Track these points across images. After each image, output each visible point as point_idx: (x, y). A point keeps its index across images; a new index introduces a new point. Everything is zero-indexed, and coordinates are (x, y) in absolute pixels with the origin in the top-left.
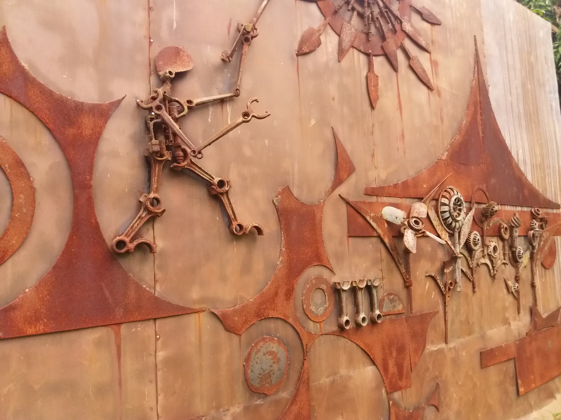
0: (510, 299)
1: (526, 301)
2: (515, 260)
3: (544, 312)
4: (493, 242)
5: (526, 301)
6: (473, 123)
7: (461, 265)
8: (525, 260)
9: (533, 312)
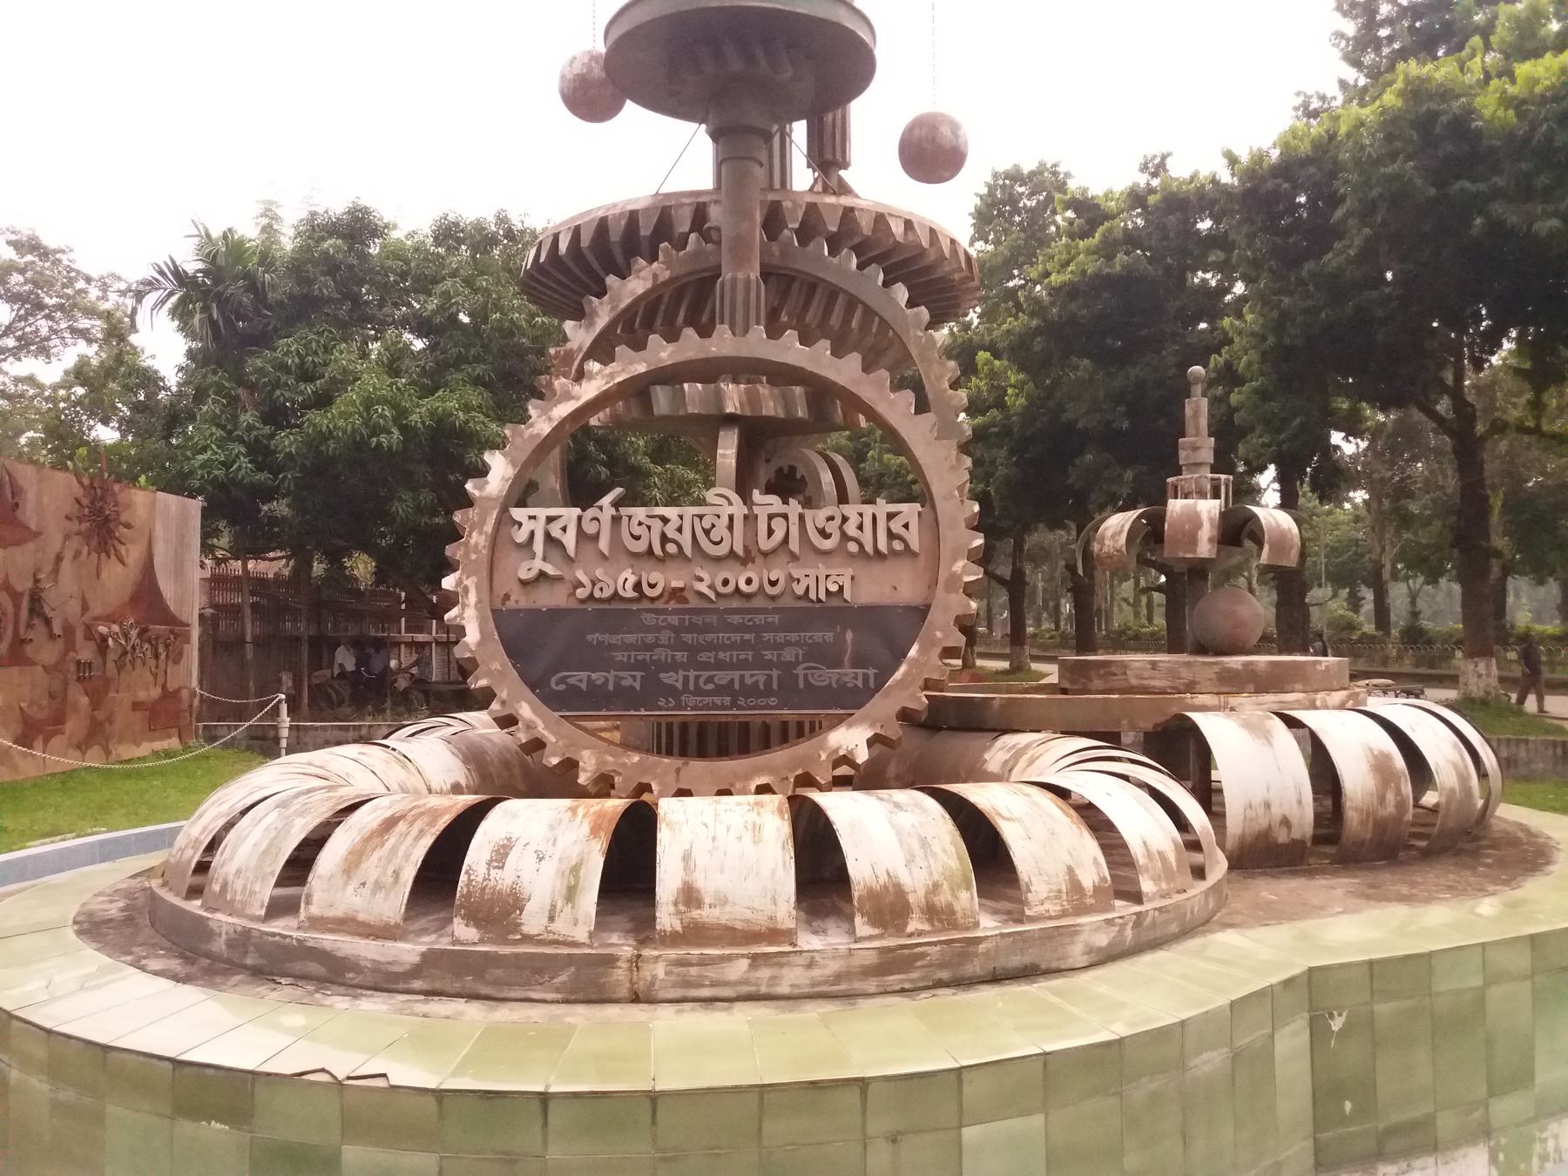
1: (161, 680)
2: (157, 656)
3: (171, 687)
4: (146, 646)
5: (161, 680)
8: (163, 657)
9: (164, 687)
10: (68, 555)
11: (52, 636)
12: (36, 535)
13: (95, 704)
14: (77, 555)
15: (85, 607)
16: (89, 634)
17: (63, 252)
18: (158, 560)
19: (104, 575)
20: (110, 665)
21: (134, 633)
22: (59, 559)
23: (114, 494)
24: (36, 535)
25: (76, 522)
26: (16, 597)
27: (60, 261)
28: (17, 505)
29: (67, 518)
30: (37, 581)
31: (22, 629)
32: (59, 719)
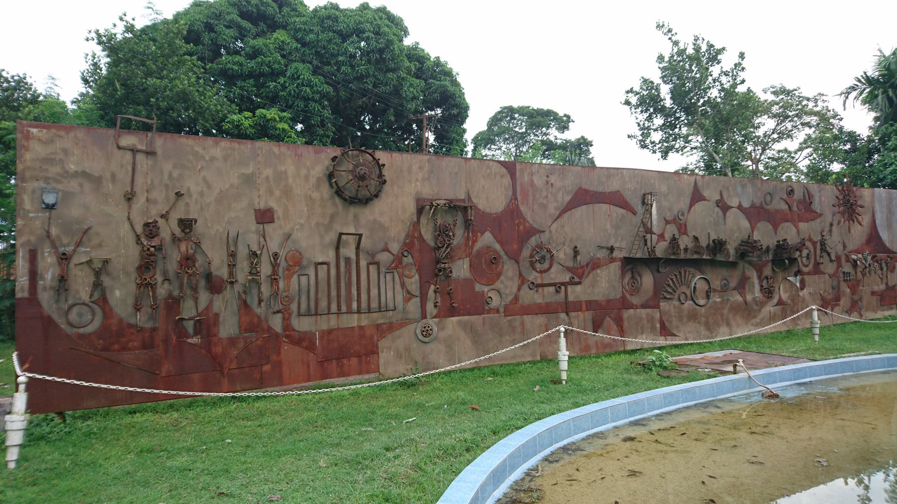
0: (880, 279)
1: (885, 281)
2: (882, 269)
3: (890, 284)
4: (876, 264)
5: (885, 281)
6: (872, 232)
7: (868, 269)
8: (885, 269)
9: (887, 284)
10: (835, 223)
11: (831, 261)
12: (821, 215)
13: (853, 292)
14: (839, 223)
15: (845, 247)
16: (848, 260)
17: (796, 90)
18: (878, 222)
19: (852, 231)
20: (859, 274)
21: (869, 258)
22: (831, 225)
23: (853, 192)
24: (821, 215)
25: (837, 207)
26: (814, 244)
27: (795, 94)
28: (811, 202)
29: (833, 206)
30: (823, 236)
31: (818, 258)
32: (837, 299)
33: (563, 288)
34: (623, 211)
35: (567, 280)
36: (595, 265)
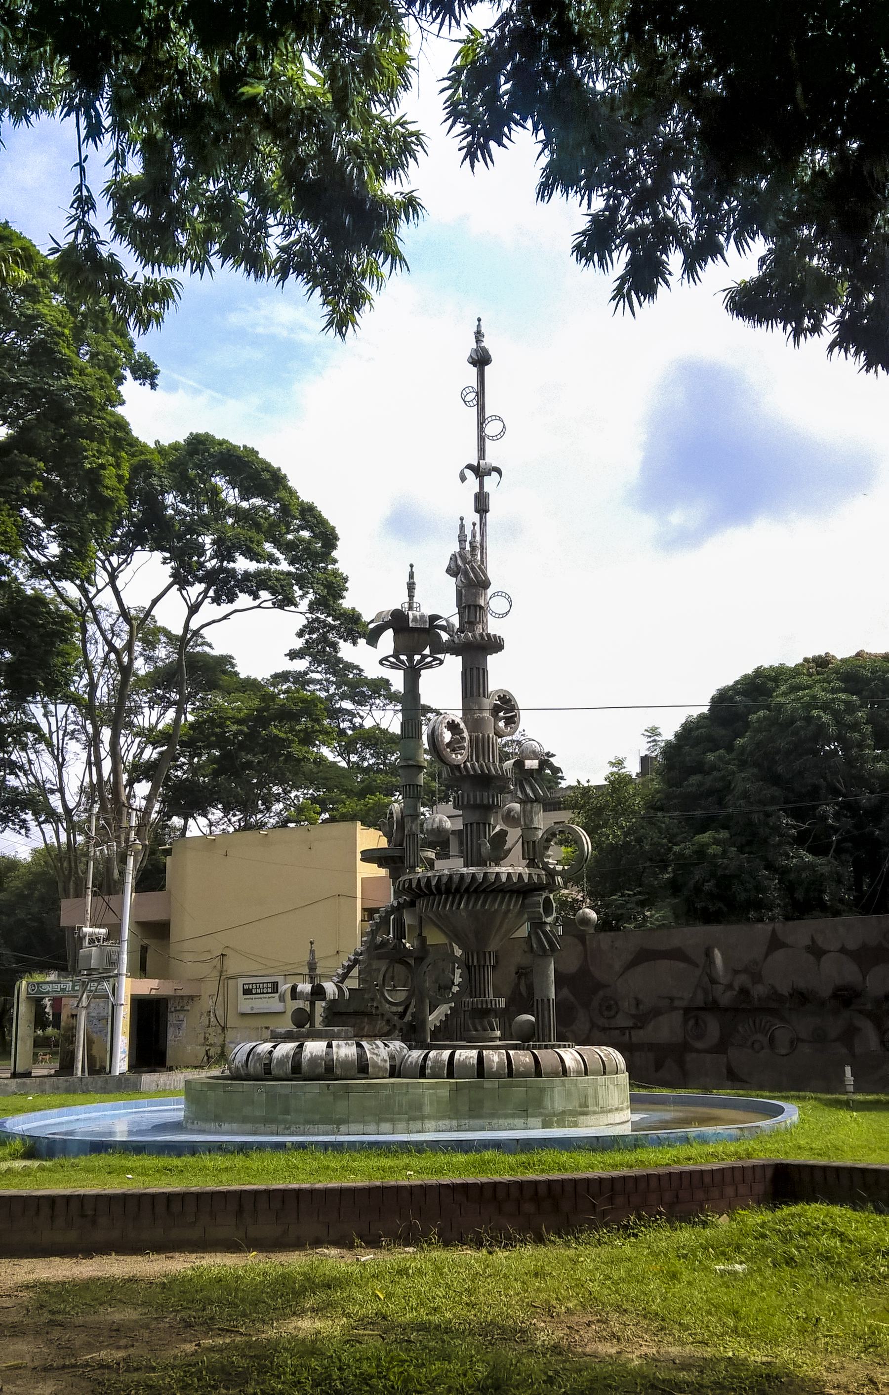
33: (627, 1032)
34: (682, 965)
35: (631, 1025)
36: (656, 1012)
